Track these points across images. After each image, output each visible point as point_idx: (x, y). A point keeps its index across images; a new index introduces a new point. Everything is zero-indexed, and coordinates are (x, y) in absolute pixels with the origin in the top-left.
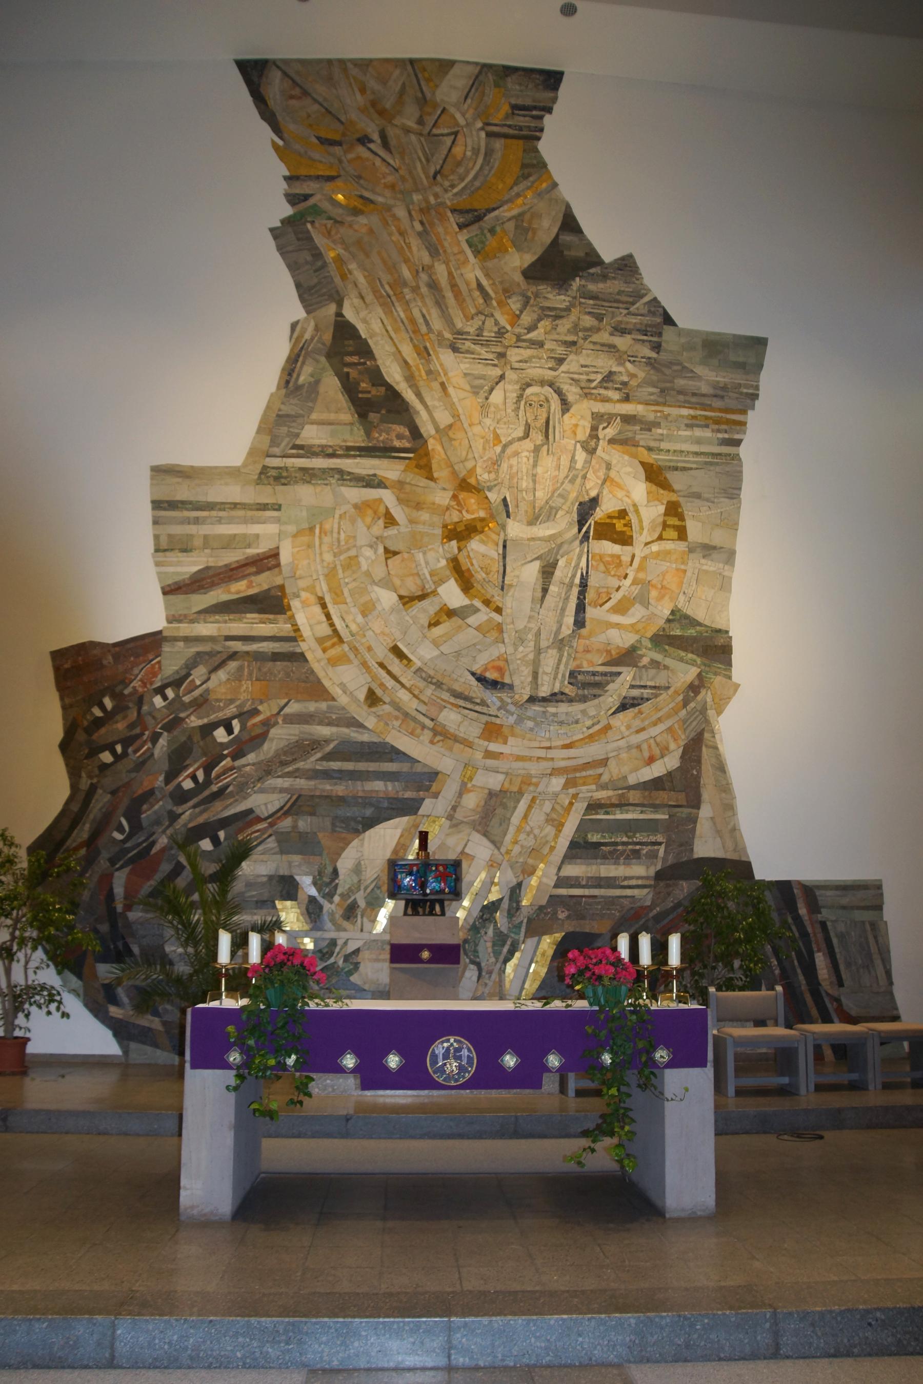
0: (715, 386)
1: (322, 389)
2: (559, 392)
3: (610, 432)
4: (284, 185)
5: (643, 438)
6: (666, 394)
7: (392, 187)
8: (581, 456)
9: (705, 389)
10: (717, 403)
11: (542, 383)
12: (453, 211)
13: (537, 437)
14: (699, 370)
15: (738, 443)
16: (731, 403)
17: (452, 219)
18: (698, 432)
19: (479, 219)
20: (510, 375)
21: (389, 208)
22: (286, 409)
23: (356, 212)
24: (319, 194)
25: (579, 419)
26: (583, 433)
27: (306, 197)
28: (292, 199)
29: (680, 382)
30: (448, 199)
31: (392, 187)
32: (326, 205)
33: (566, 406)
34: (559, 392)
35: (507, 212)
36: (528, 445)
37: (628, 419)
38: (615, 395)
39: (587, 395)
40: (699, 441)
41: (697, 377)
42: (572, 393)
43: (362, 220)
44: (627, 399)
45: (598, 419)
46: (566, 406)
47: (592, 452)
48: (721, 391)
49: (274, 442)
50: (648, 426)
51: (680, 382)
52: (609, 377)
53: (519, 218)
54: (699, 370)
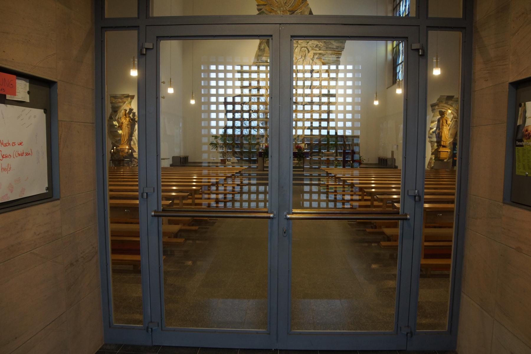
0: (337, 46)
1: (266, 49)
2: (308, 49)
3: (316, 57)
4: (257, 7)
5: (323, 58)
6: (327, 48)
7: (277, 6)
8: (311, 61)
9: (335, 47)
10: (337, 50)
11: (304, 47)
12: (289, 11)
13: (303, 58)
14: (334, 43)
15: (340, 58)
16: (339, 50)
17: (288, 13)
18: (333, 56)
19: (294, 13)
20: (299, 46)
21: (276, 11)
22: (260, 54)
23: (270, 12)
24: (264, 8)
25: (312, 52)
26: (311, 57)
27: (261, 9)
28: (259, 10)
29: (330, 46)
30: (288, 9)
31: (277, 6)
32: (265, 11)
33: (309, 52)
34: (308, 49)
35: (299, 11)
36: (302, 59)
37: (320, 54)
38: (318, 49)
39: (313, 49)
40: (333, 58)
41: (333, 45)
42: (310, 49)
43: (272, 14)
44: (320, 50)
45: (315, 54)
46: (309, 52)
47: (313, 60)
48: (338, 47)
49: (258, 60)
50: (323, 55)
51: (330, 46)
52: (317, 46)
53: (301, 12)
54: (334, 43)
